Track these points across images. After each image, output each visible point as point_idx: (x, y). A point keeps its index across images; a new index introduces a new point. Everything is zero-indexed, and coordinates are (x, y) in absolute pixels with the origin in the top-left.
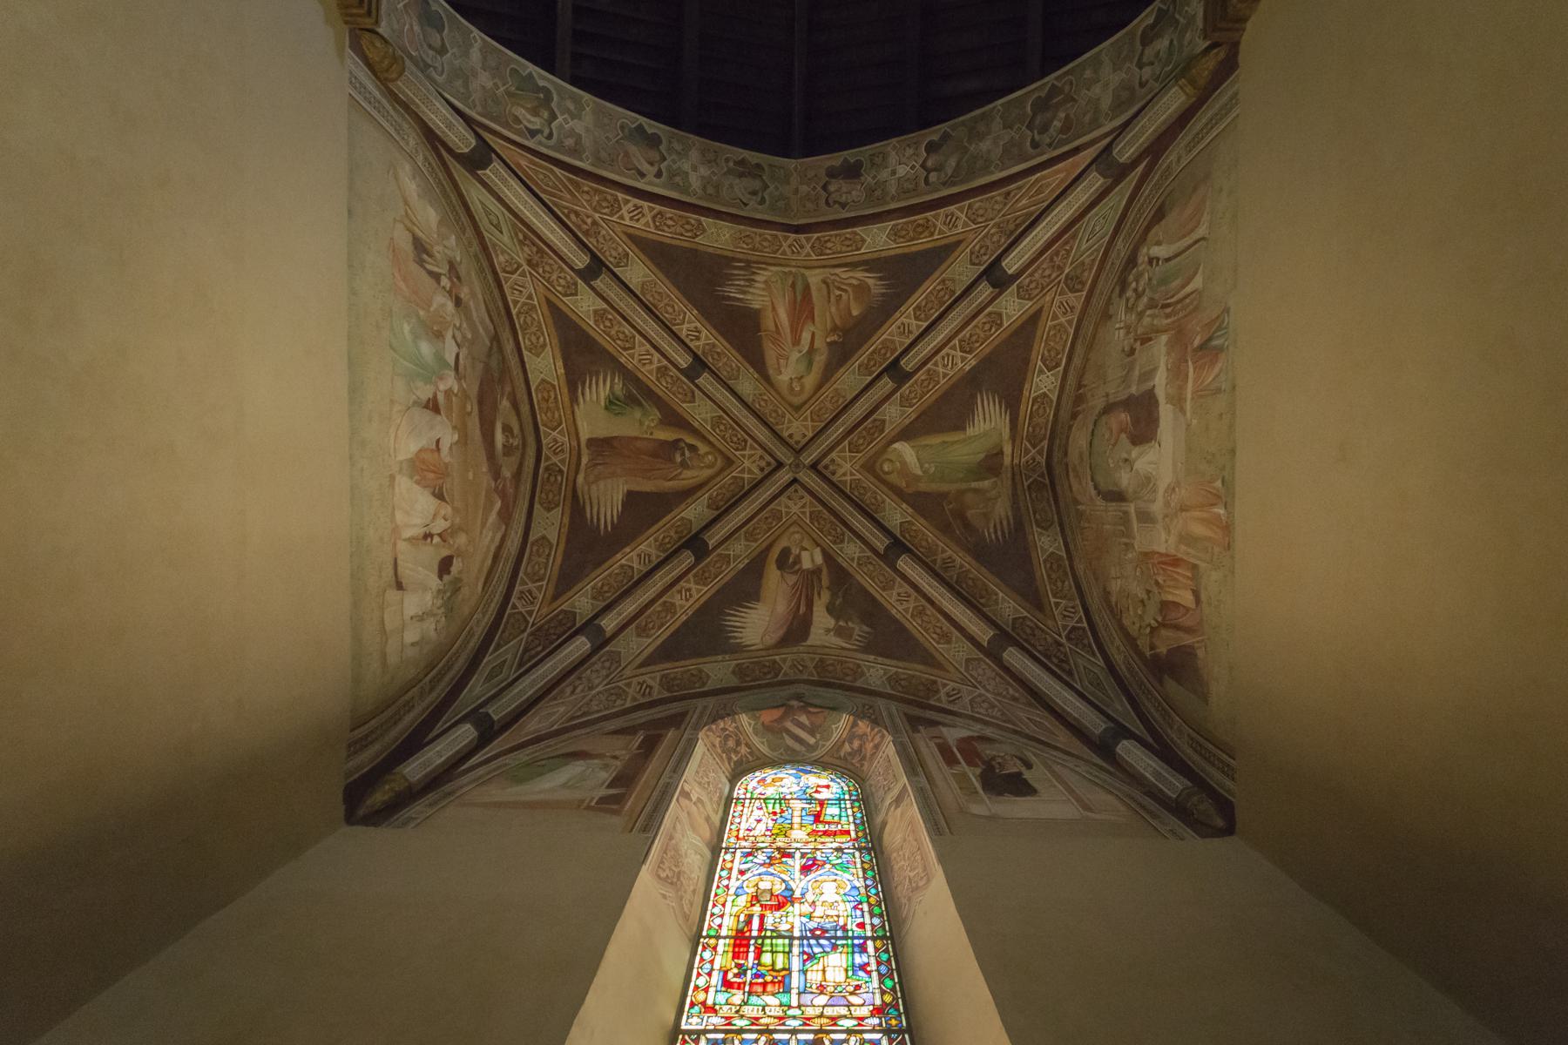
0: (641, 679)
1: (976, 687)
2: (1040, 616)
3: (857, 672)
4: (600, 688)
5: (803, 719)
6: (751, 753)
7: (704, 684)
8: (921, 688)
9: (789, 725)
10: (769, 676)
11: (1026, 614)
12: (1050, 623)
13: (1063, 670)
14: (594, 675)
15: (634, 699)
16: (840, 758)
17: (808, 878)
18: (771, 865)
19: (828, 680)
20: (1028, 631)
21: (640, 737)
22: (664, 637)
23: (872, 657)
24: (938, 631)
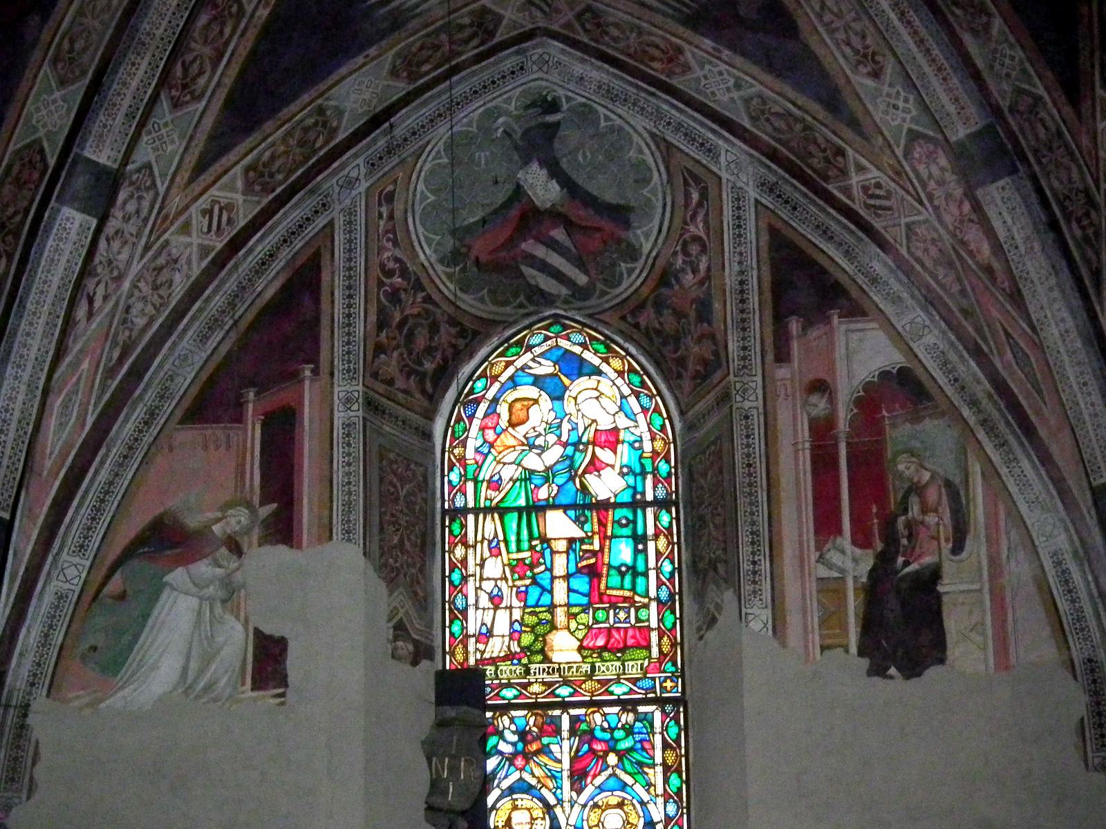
0: (203, 203)
1: (921, 203)
2: (1068, 110)
3: (673, 56)
4: (136, 268)
5: (559, 234)
6: (463, 333)
7: (334, 131)
8: (812, 148)
9: (529, 246)
10: (475, 42)
11: (1041, 91)
12: (1085, 141)
13: (1087, 261)
14: (116, 245)
15: (205, 251)
16: (637, 326)
17: (583, 799)
18: (527, 757)
19: (610, 51)
20: (1042, 132)
21: (254, 432)
22: (228, 82)
23: (708, 43)
24: (856, 41)
